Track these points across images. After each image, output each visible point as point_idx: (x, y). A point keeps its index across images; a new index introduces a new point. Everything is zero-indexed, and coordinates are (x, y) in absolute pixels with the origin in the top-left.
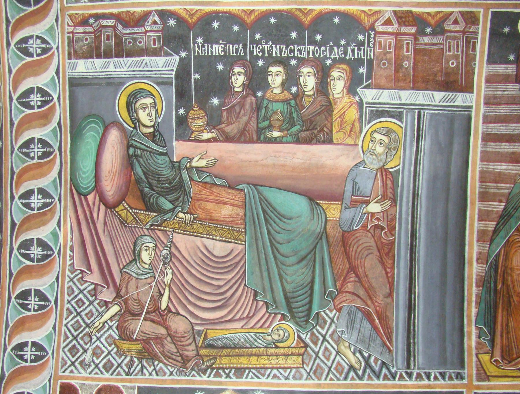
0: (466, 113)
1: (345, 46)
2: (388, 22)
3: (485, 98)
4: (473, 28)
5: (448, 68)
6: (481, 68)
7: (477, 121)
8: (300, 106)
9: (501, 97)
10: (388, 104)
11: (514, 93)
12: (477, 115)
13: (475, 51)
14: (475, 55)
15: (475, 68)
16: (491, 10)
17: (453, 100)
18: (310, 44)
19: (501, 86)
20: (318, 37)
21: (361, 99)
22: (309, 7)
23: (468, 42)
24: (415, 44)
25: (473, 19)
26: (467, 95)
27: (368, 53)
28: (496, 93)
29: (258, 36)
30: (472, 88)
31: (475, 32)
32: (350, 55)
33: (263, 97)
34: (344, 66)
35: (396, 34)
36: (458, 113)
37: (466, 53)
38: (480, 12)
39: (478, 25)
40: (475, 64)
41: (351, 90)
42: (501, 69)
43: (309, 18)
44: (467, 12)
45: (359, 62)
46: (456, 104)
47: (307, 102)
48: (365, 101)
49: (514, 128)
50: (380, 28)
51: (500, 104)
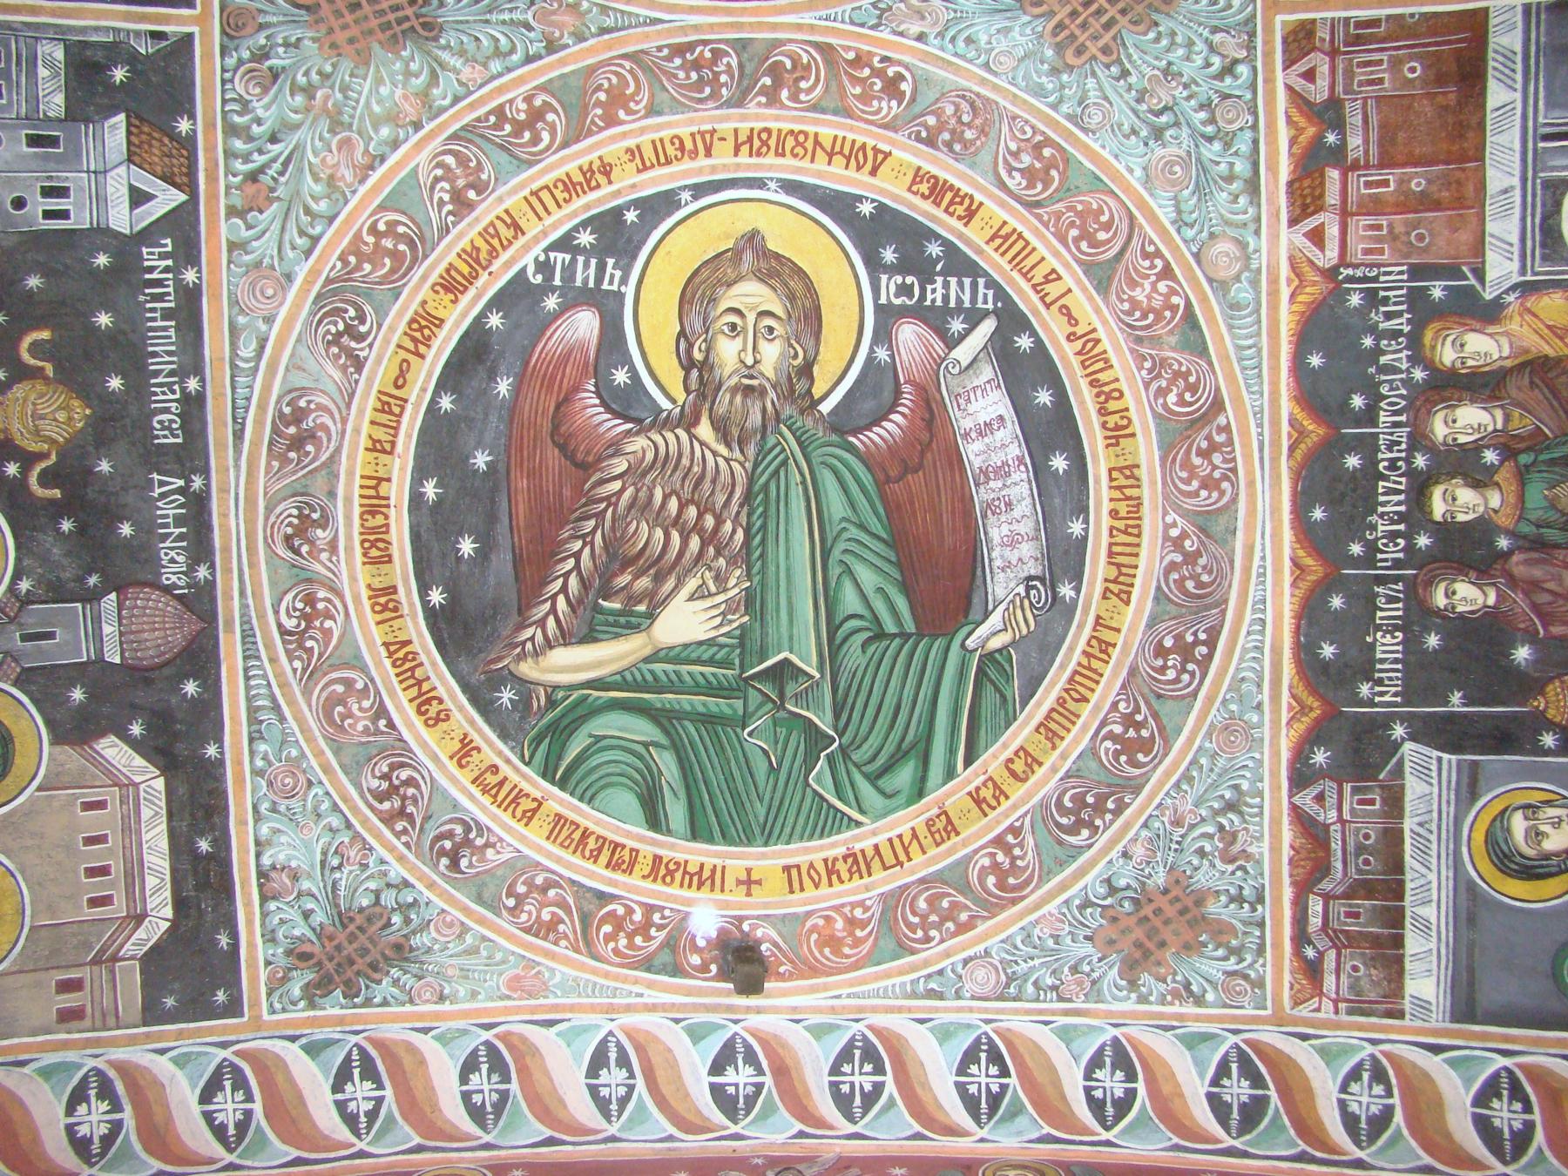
0: (1543, 17)
1: (1379, 335)
2: (1317, 236)
4: (1323, 34)
5: (1424, 81)
8: (1536, 441)
10: (1523, 219)
13: (1379, 20)
14: (1389, 17)
15: (1421, 14)
17: (1508, 56)
18: (1373, 422)
20: (1357, 401)
21: (1513, 288)
22: (1285, 428)
23: (1357, 40)
24: (1367, 166)
25: (1301, 35)
26: (1492, 22)
27: (1394, 279)
29: (1356, 549)
31: (1333, 26)
32: (1402, 324)
33: (1511, 534)
34: (1428, 336)
35: (1345, 214)
36: (1542, 39)
37: (1383, 41)
38: (1284, 23)
39: (1313, 21)
40: (1412, 15)
41: (1488, 314)
43: (1309, 425)
44: (1284, 52)
45: (1416, 298)
46: (1518, 48)
47: (1522, 423)
48: (1516, 279)
50: (1332, 254)
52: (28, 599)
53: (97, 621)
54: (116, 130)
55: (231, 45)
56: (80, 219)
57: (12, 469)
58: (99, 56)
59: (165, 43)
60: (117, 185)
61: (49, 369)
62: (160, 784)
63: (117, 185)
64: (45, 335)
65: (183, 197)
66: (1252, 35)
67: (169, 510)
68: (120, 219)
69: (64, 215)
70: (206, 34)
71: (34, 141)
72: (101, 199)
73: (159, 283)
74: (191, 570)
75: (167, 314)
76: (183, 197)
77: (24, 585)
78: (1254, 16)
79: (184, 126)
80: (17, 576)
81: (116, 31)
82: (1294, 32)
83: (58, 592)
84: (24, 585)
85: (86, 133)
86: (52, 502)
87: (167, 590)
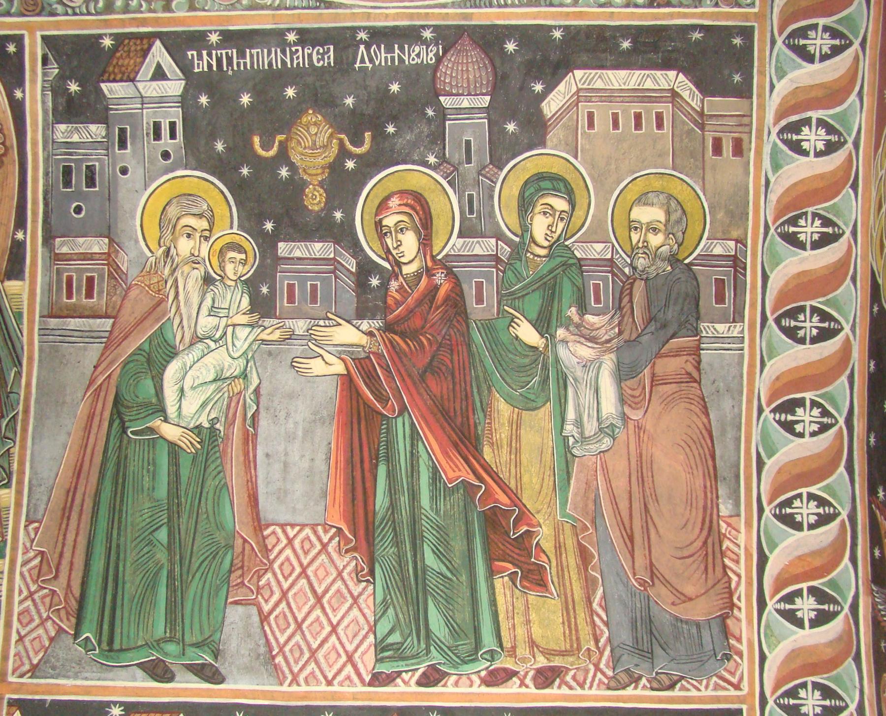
52: (443, 159)
53: (459, 111)
54: (112, 90)
55: (48, 9)
56: (176, 114)
57: (350, 164)
58: (62, 100)
59: (50, 56)
60: (151, 89)
61: (280, 138)
62: (579, 73)
63: (151, 89)
64: (256, 140)
65: (158, 43)
67: (382, 57)
68: (175, 87)
69: (173, 125)
70: (42, 27)
71: (123, 145)
72: (161, 100)
73: (219, 61)
74: (426, 43)
75: (242, 55)
76: (158, 43)
77: (432, 159)
79: (107, 42)
80: (425, 164)
81: (44, 89)
83: (437, 138)
84: (432, 159)
85: (117, 110)
86: (373, 138)
87: (439, 60)
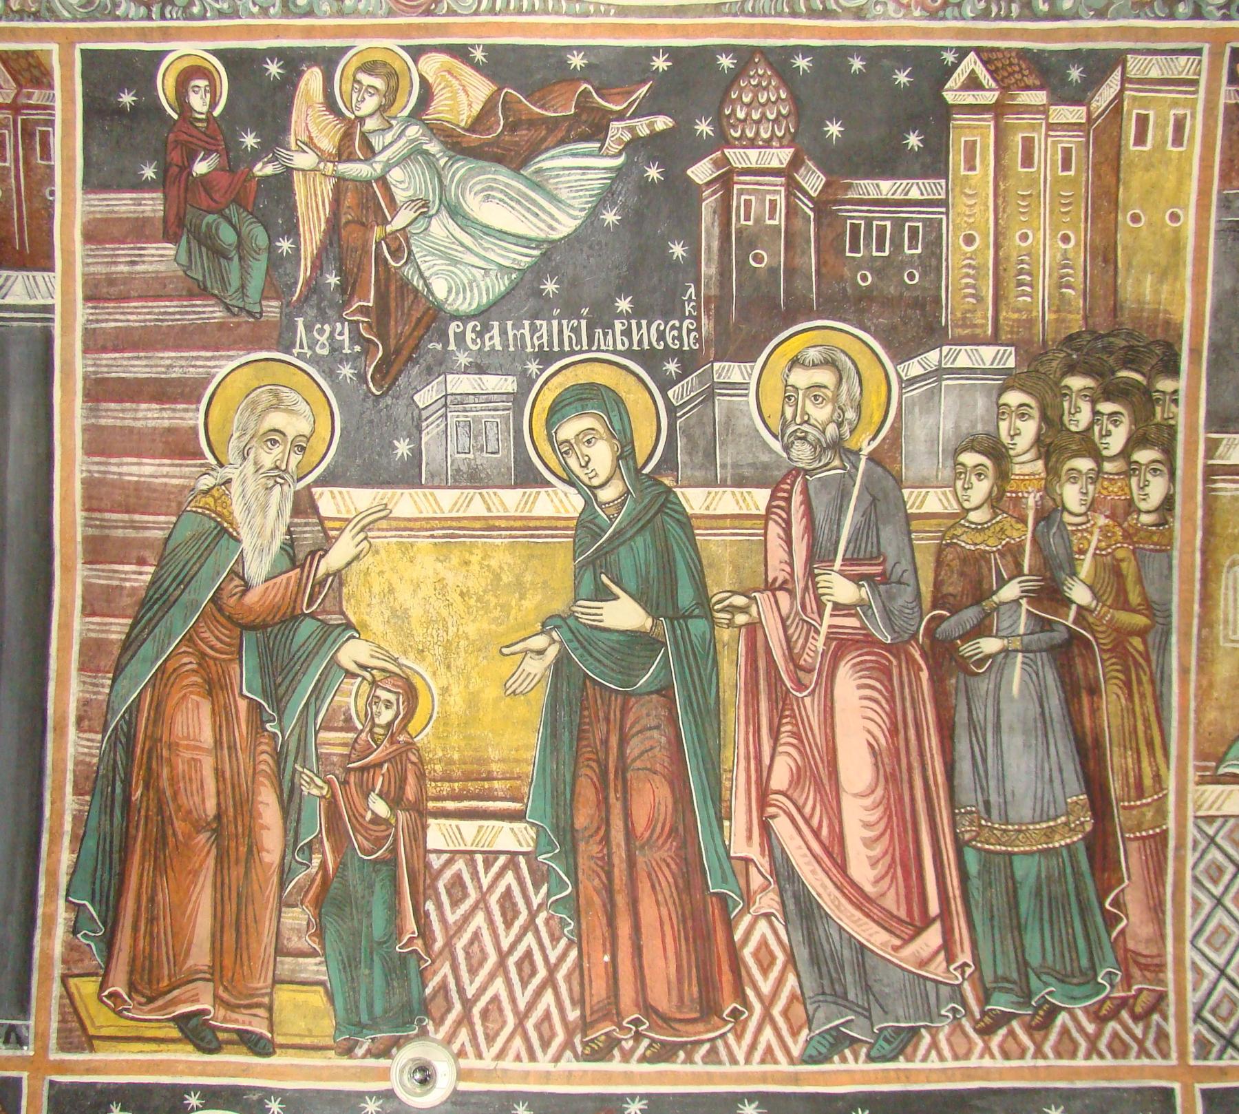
0: (39, 324)
3: (85, 284)
4: (37, 97)
6: (69, 202)
7: (68, 347)
9: (129, 279)
11: (162, 267)
12: (68, 329)
13: (49, 159)
14: (51, 168)
15: (52, 202)
16: (79, 47)
19: (125, 251)
23: (28, 134)
25: (36, 73)
26: (39, 275)
28: (113, 269)
30: (51, 257)
31: (45, 108)
36: (15, 324)
37: (26, 162)
38: (49, 52)
39: (51, 87)
40: (52, 193)
42: (123, 204)
44: (16, 52)
49: (168, 362)
51: (127, 299)
66: (36, 16)
78: (58, 19)
82: (39, 65)
